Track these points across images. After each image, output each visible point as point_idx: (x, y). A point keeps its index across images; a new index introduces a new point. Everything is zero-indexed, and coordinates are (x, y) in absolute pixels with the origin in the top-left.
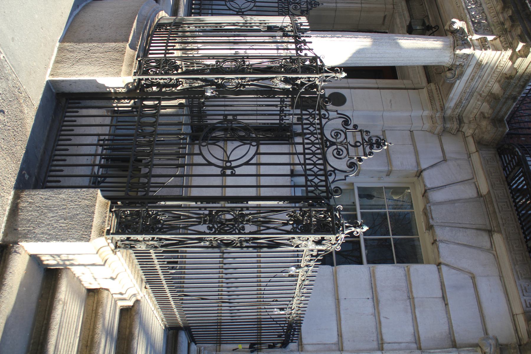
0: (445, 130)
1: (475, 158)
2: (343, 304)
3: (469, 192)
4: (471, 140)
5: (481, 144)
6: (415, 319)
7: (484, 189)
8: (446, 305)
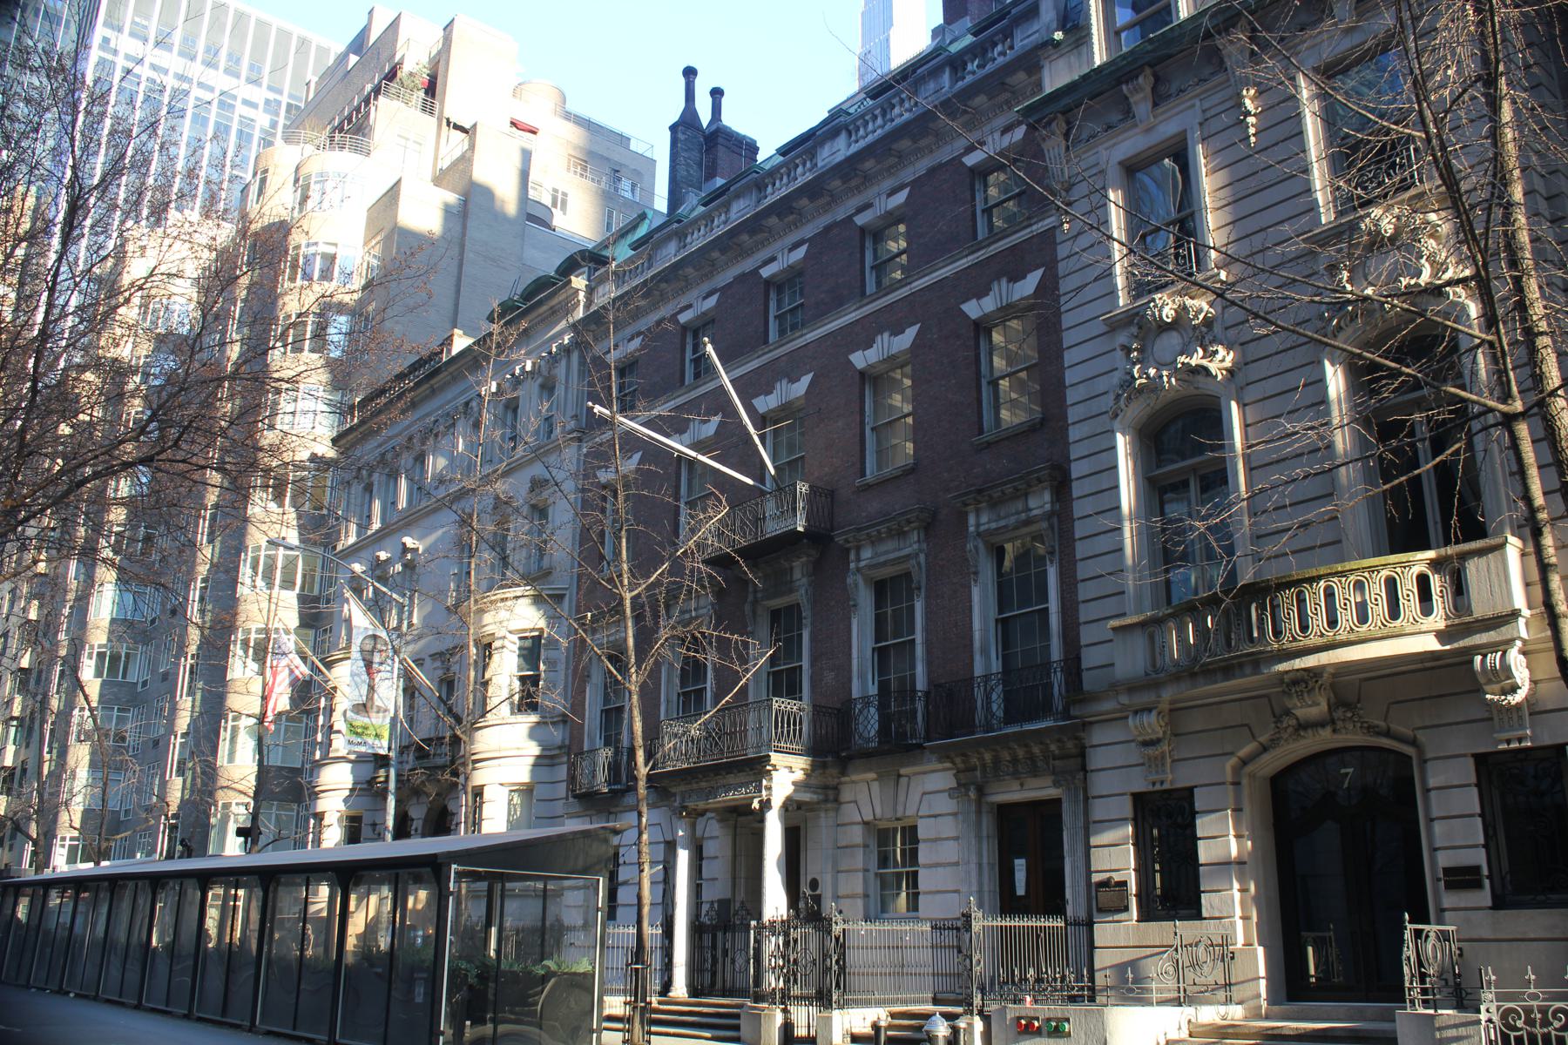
0: (836, 800)
1: (855, 777)
2: (939, 888)
3: (875, 786)
4: (843, 779)
5: (843, 773)
6: (947, 839)
7: (872, 775)
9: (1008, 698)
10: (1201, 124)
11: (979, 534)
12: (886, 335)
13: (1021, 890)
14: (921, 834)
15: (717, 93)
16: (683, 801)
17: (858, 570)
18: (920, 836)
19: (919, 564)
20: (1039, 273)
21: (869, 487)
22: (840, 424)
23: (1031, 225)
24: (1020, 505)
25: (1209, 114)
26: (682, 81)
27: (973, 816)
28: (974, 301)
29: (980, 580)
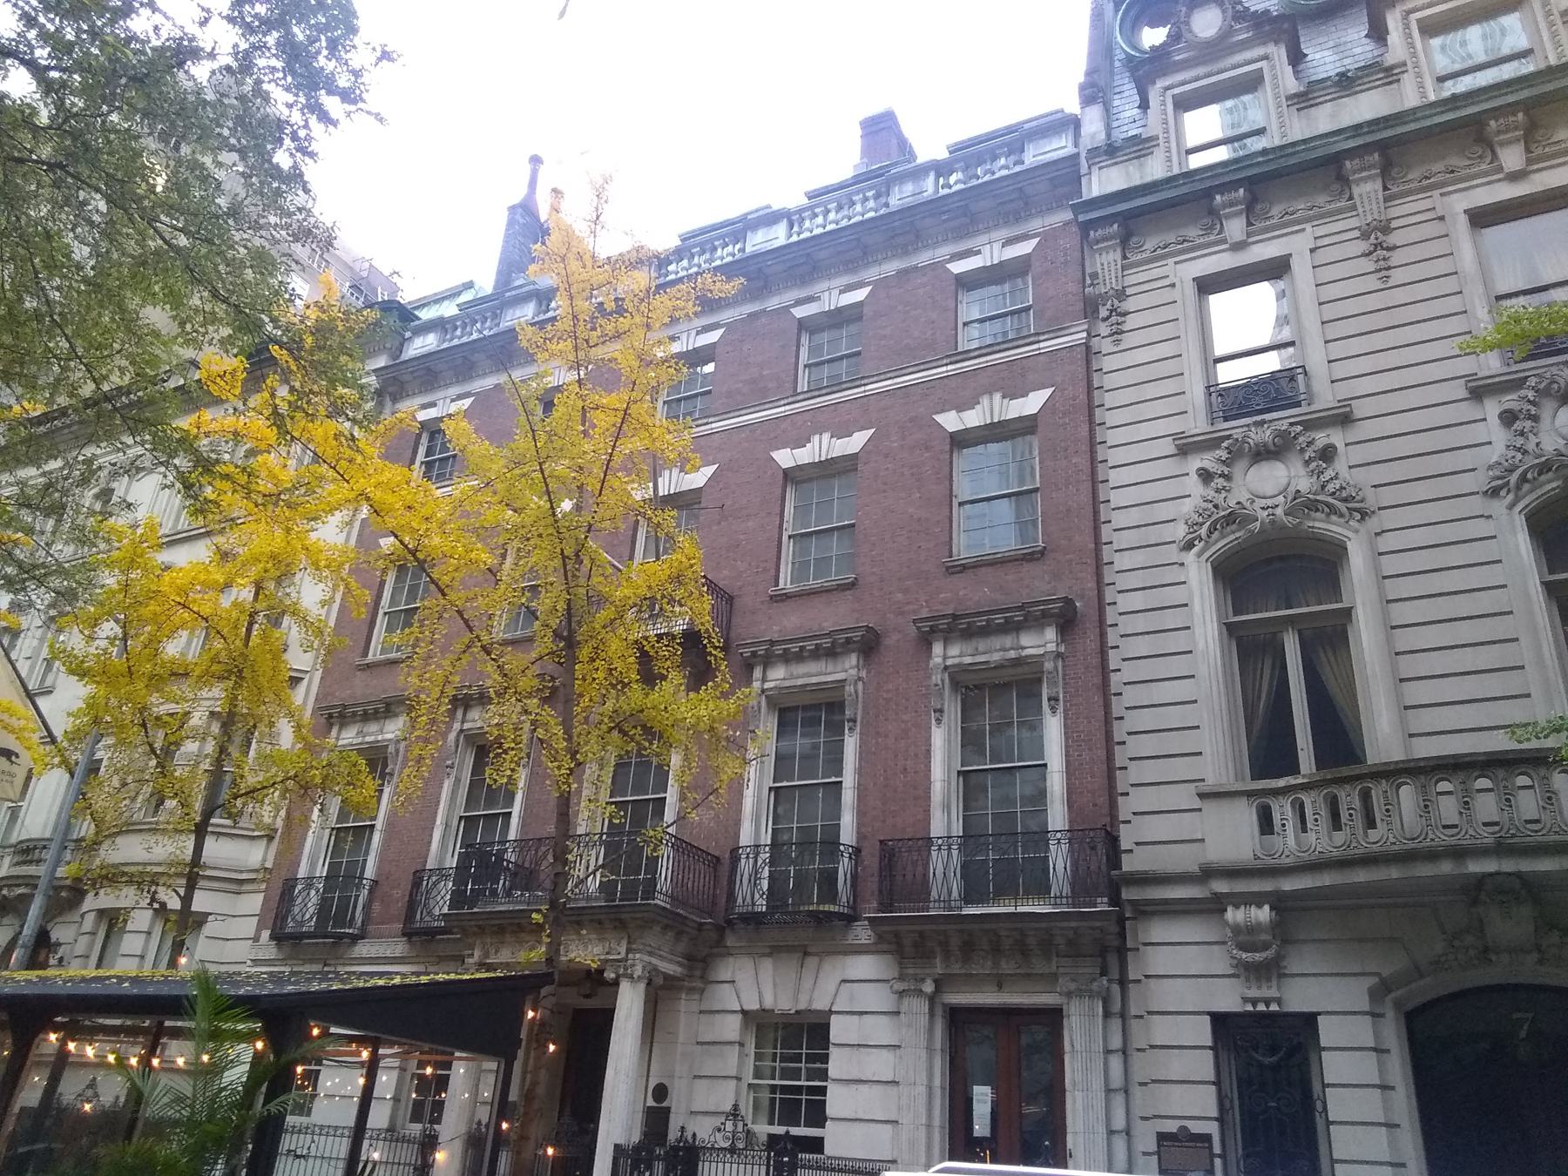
4: (715, 950)
8: (866, 1013)
9: (970, 873)
10: (1312, 251)
11: (946, 668)
12: (826, 436)
13: (981, 1128)
14: (835, 1034)
15: (556, 192)
16: (487, 955)
17: (763, 691)
18: (833, 1039)
19: (856, 692)
20: (1047, 392)
21: (786, 597)
22: (750, 524)
23: (1039, 342)
24: (1008, 641)
25: (1320, 243)
26: (527, 169)
27: (924, 1020)
28: (953, 413)
29: (945, 720)
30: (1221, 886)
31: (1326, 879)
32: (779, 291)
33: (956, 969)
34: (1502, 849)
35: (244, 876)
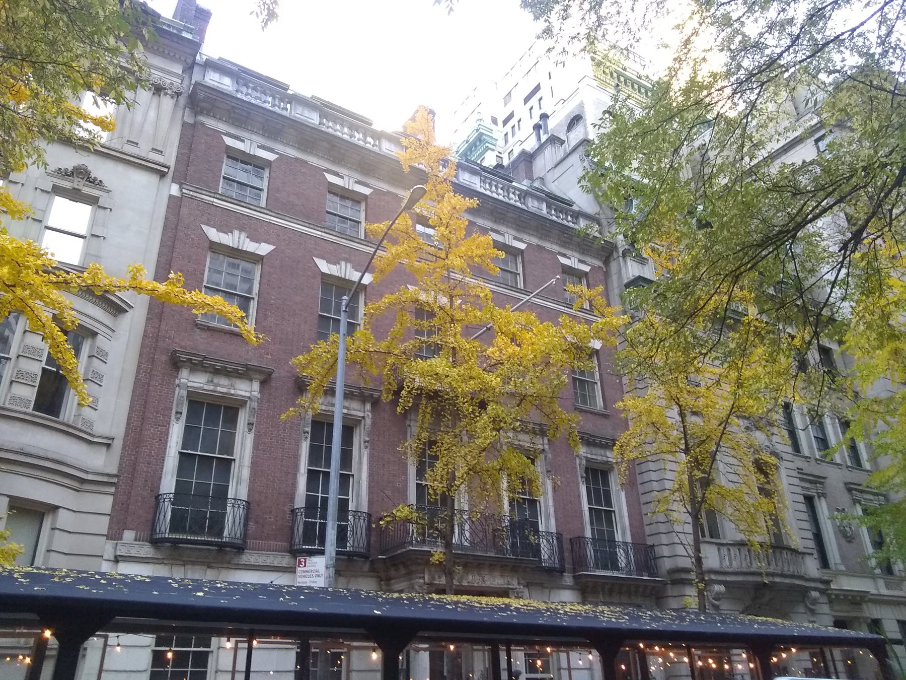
24: (602, 452)
30: (713, 577)
31: (740, 578)
32: (483, 218)
33: (608, 599)
34: (782, 575)
35: (90, 477)
